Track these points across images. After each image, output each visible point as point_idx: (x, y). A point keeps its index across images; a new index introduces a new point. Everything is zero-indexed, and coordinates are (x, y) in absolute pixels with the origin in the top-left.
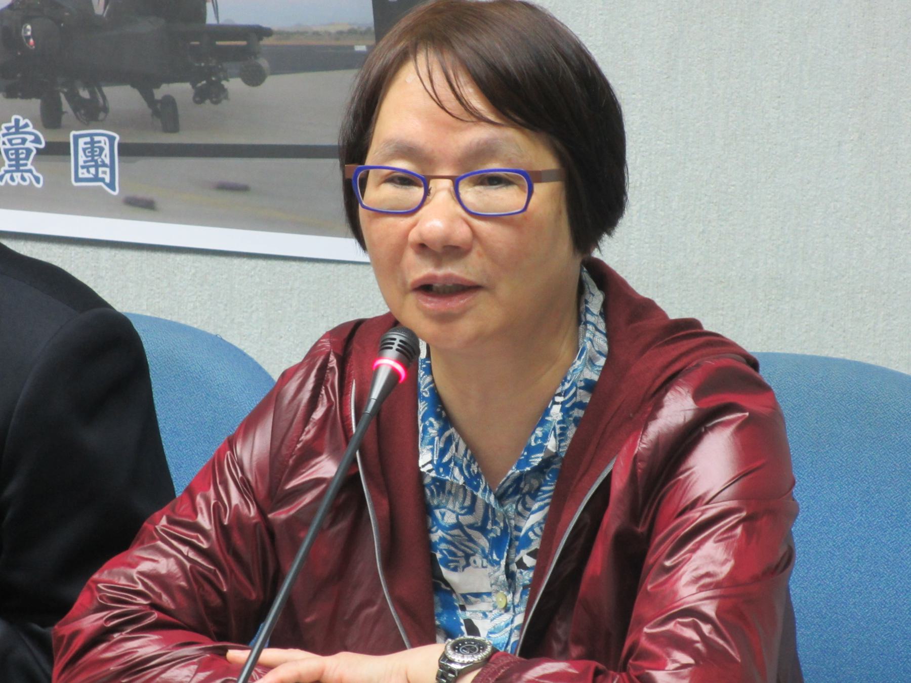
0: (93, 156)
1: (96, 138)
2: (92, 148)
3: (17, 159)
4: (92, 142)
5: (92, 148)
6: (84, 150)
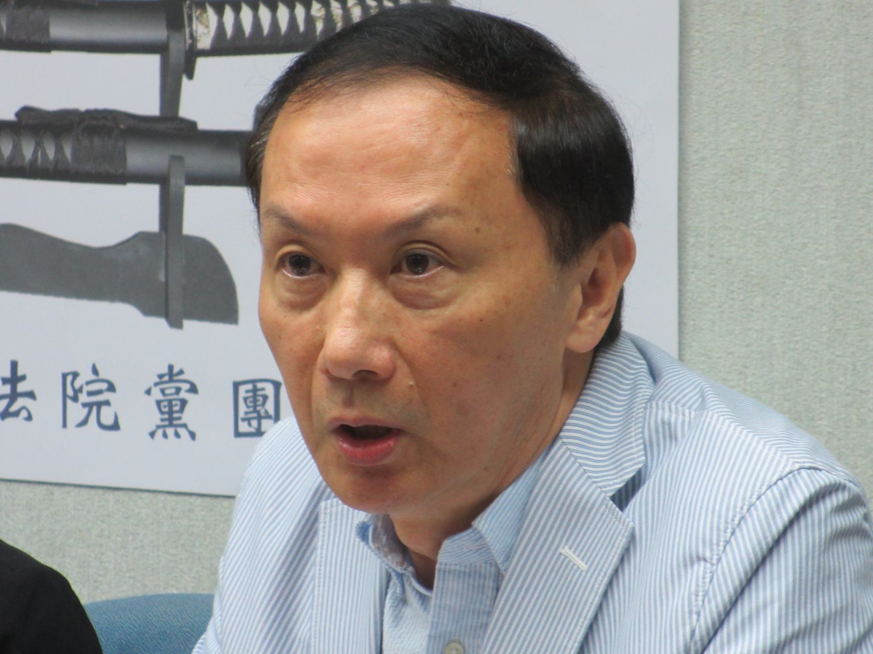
0: (255, 406)
1: (260, 385)
2: (255, 396)
3: (171, 412)
4: (255, 390)
5: (255, 396)
6: (245, 399)
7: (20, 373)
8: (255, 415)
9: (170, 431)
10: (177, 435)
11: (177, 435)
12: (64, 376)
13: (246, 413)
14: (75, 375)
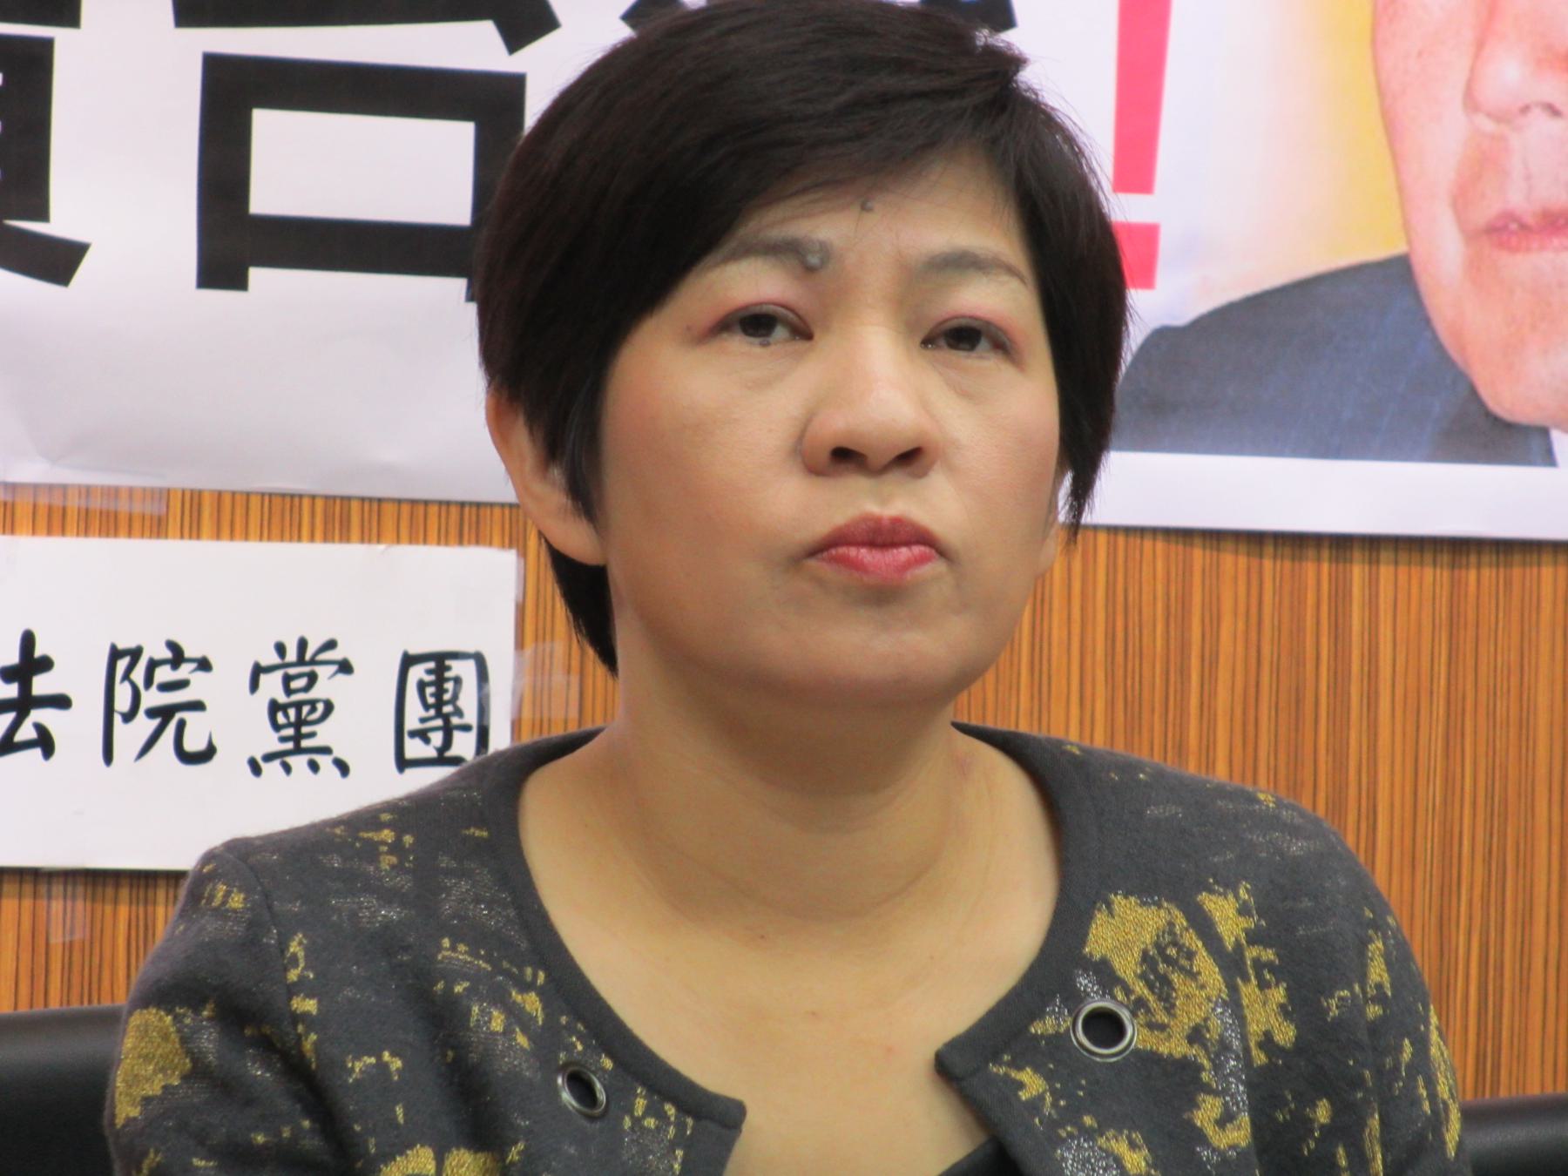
0: (439, 704)
6: (422, 686)
7: (38, 652)
8: (439, 722)
9: (299, 762)
10: (314, 767)
11: (314, 767)
12: (115, 654)
13: (423, 720)
14: (135, 654)
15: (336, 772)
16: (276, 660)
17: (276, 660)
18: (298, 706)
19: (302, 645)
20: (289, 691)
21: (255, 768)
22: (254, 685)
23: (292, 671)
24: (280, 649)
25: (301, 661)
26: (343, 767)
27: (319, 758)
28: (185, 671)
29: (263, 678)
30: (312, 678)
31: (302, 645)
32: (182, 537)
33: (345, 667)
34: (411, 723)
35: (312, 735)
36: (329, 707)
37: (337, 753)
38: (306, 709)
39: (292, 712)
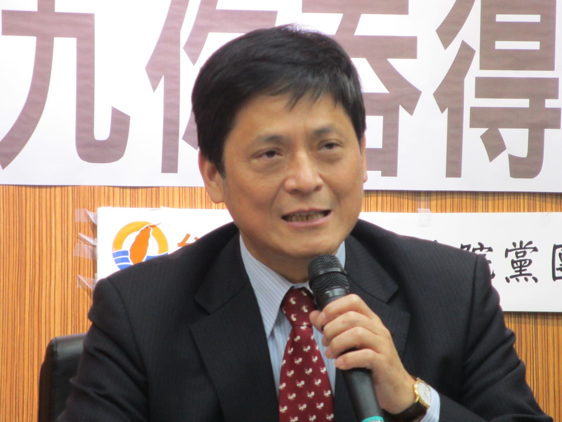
9: (521, 278)
10: (526, 280)
11: (526, 280)
15: (534, 281)
16: (513, 248)
17: (513, 248)
18: (521, 261)
19: (521, 243)
20: (517, 257)
21: (508, 280)
22: (506, 255)
23: (518, 251)
24: (514, 244)
25: (521, 248)
26: (536, 280)
27: (527, 277)
28: (484, 252)
29: (509, 253)
30: (525, 253)
31: (521, 243)
32: (483, 212)
33: (535, 249)
34: (557, 266)
35: (525, 270)
36: (530, 262)
37: (533, 276)
38: (523, 262)
39: (519, 263)
